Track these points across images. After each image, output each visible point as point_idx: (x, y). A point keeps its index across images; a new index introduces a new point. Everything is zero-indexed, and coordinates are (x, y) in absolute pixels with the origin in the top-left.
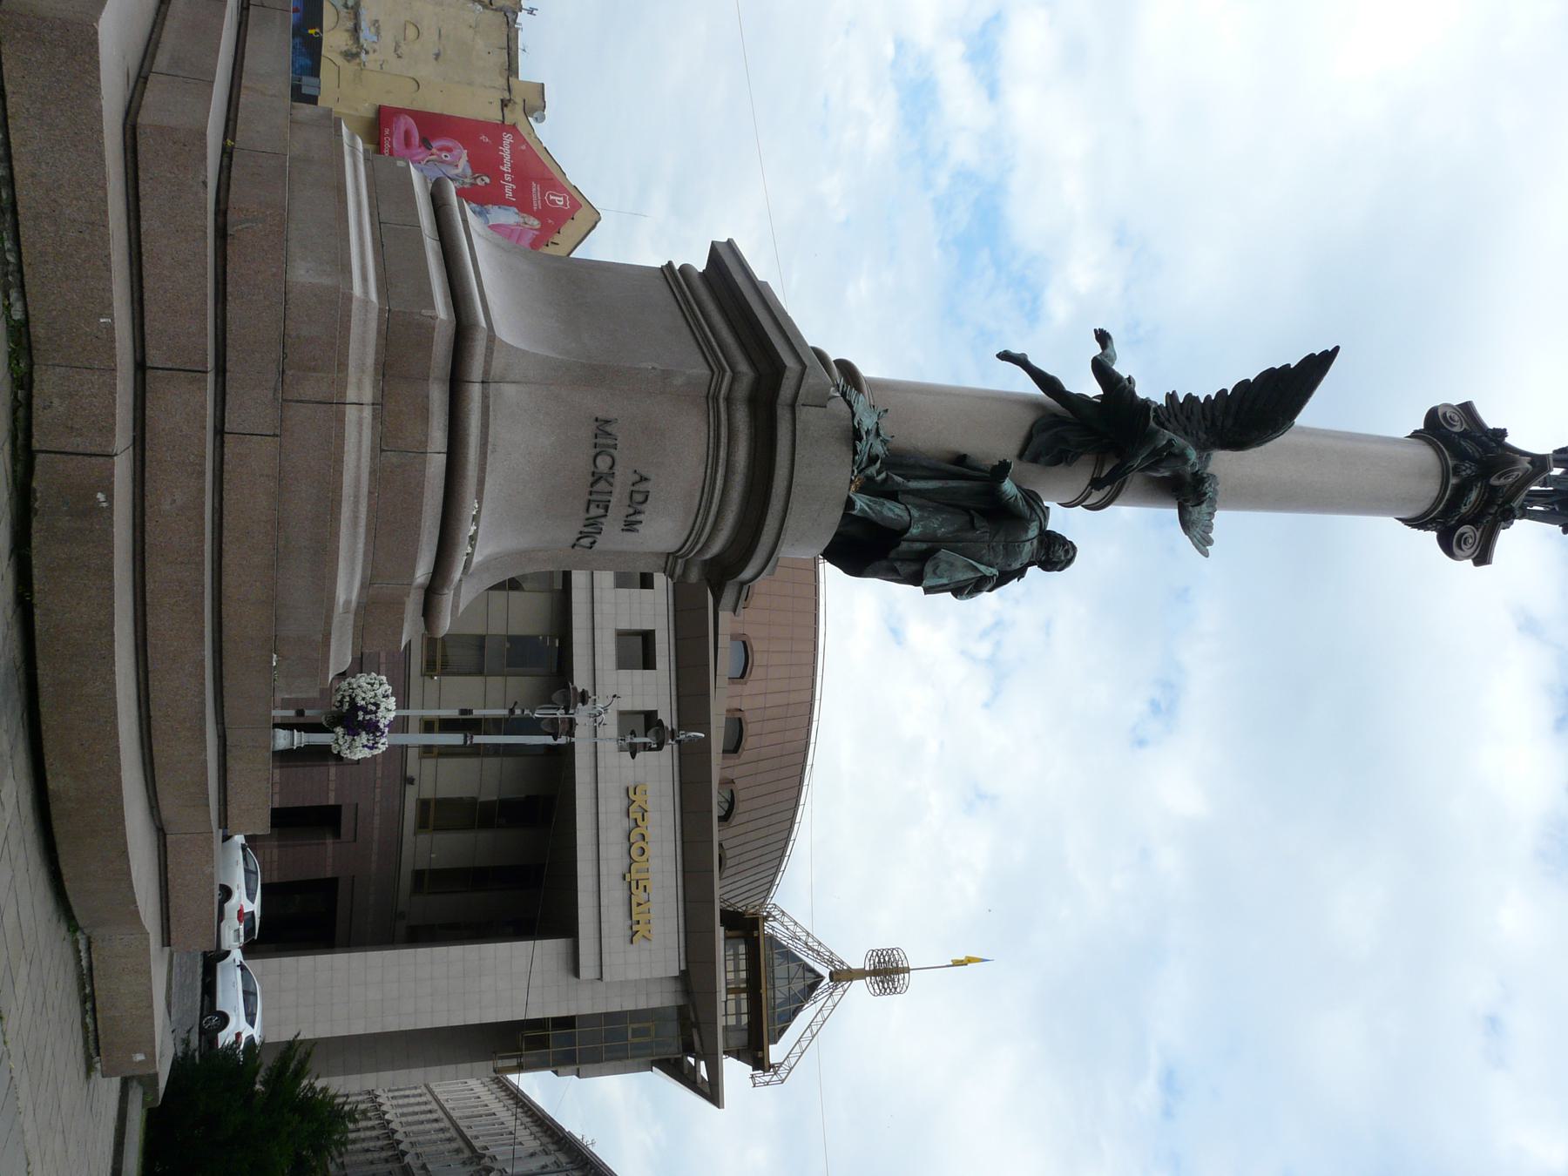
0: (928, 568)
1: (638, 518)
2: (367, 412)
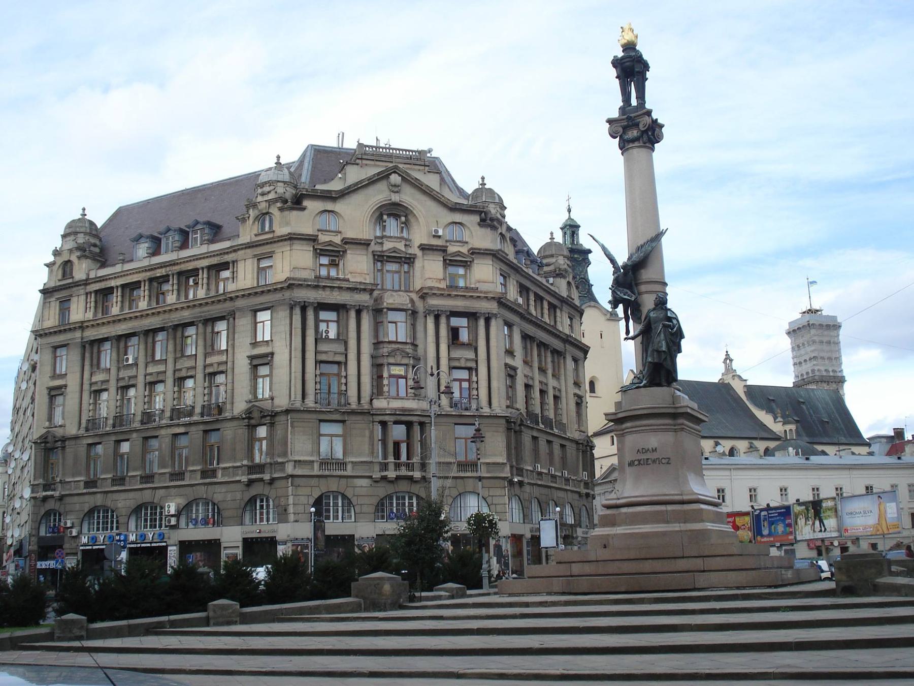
0: (660, 350)
1: (650, 449)
2: (618, 528)
